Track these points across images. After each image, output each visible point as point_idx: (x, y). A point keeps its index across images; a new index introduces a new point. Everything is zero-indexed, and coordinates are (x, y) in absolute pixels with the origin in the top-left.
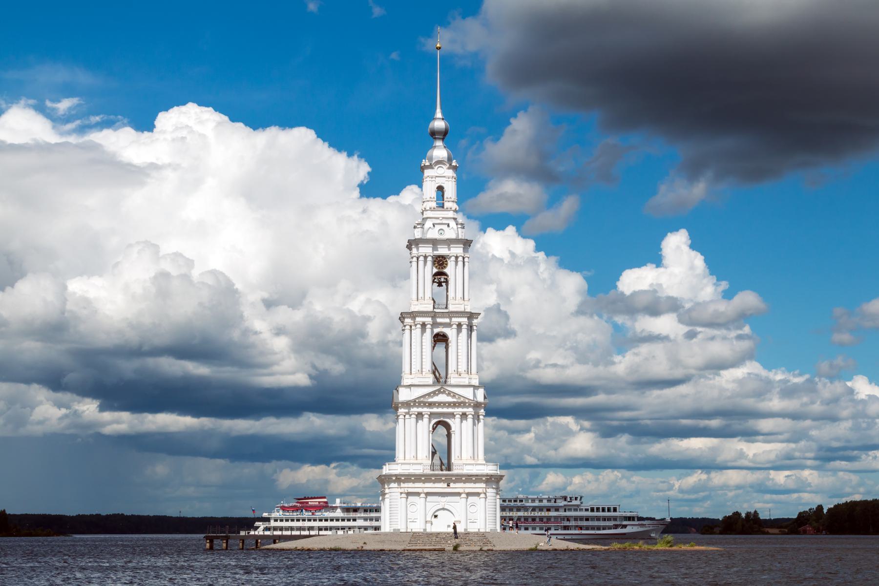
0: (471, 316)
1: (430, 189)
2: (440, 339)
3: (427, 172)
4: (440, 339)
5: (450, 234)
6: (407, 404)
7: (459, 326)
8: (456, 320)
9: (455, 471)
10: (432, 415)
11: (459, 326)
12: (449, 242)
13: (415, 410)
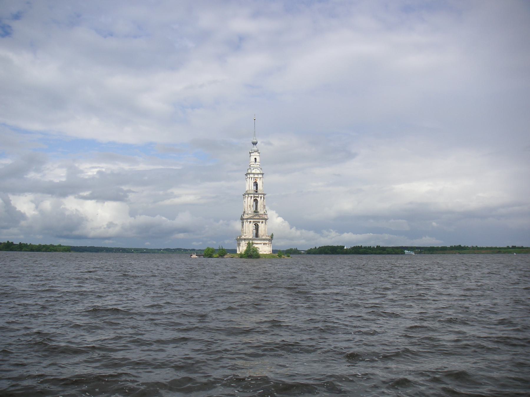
0: (264, 195)
1: (253, 159)
2: (256, 201)
3: (252, 154)
4: (256, 201)
5: (258, 172)
6: (247, 219)
7: (261, 197)
8: (260, 196)
9: (260, 237)
10: (254, 222)
11: (261, 197)
12: (258, 174)
13: (249, 220)
